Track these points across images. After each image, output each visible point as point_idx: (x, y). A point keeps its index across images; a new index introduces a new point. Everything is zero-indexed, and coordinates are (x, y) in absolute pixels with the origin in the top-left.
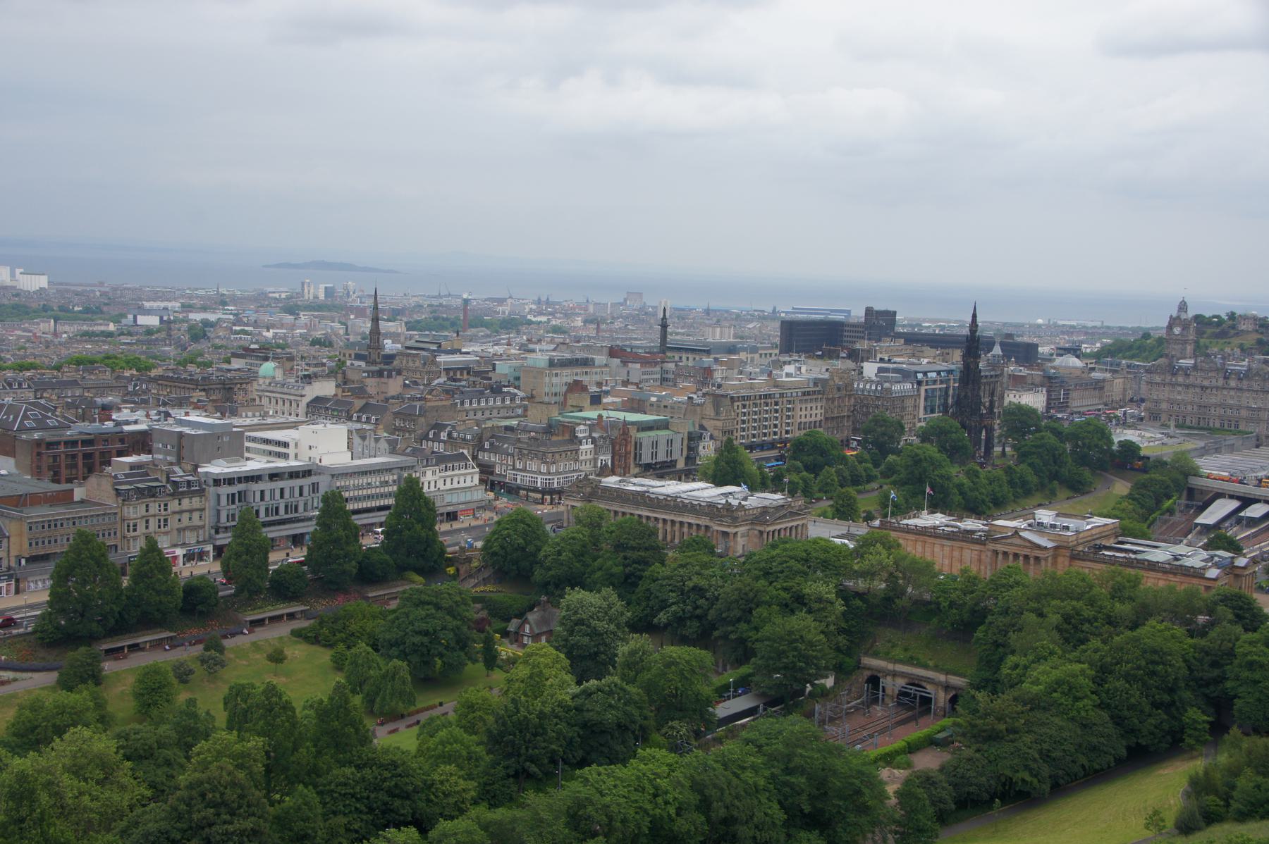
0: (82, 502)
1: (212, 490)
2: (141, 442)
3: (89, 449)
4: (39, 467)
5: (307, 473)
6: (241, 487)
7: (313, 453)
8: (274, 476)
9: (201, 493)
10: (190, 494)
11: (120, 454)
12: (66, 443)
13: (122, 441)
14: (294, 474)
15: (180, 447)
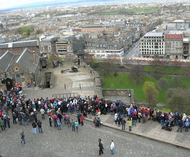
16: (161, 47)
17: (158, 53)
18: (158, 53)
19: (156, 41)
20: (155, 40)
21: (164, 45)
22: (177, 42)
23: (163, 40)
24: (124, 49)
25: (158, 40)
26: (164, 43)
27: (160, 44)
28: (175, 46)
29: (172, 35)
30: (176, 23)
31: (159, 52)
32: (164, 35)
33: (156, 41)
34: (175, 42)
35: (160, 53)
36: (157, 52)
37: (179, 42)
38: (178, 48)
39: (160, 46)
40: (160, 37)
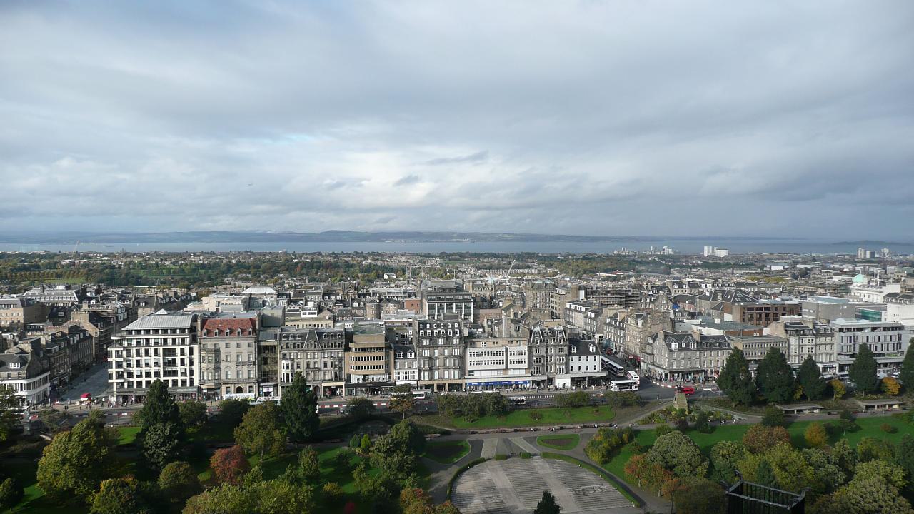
0: (767, 336)
1: (836, 334)
2: (796, 309)
3: (767, 312)
4: (744, 319)
5: (894, 329)
6: (857, 333)
7: (896, 319)
8: (874, 329)
9: (832, 334)
10: (826, 334)
11: (783, 315)
12: (758, 309)
13: (784, 309)
14: (885, 329)
15: (818, 312)
16: (187, 361)
17: (175, 382)
18: (175, 382)
19: (170, 342)
20: (165, 340)
21: (196, 356)
22: (238, 344)
23: (194, 340)
24: (52, 378)
25: (174, 340)
26: (196, 347)
27: (182, 353)
28: (233, 358)
29: (221, 322)
30: (251, 294)
31: (179, 378)
32: (195, 324)
33: (170, 342)
34: (233, 344)
35: (184, 382)
36: (170, 379)
37: (245, 343)
38: (244, 363)
39: (182, 361)
40: (183, 331)
